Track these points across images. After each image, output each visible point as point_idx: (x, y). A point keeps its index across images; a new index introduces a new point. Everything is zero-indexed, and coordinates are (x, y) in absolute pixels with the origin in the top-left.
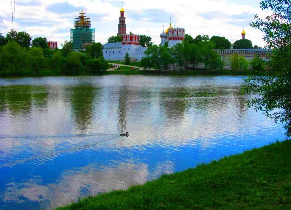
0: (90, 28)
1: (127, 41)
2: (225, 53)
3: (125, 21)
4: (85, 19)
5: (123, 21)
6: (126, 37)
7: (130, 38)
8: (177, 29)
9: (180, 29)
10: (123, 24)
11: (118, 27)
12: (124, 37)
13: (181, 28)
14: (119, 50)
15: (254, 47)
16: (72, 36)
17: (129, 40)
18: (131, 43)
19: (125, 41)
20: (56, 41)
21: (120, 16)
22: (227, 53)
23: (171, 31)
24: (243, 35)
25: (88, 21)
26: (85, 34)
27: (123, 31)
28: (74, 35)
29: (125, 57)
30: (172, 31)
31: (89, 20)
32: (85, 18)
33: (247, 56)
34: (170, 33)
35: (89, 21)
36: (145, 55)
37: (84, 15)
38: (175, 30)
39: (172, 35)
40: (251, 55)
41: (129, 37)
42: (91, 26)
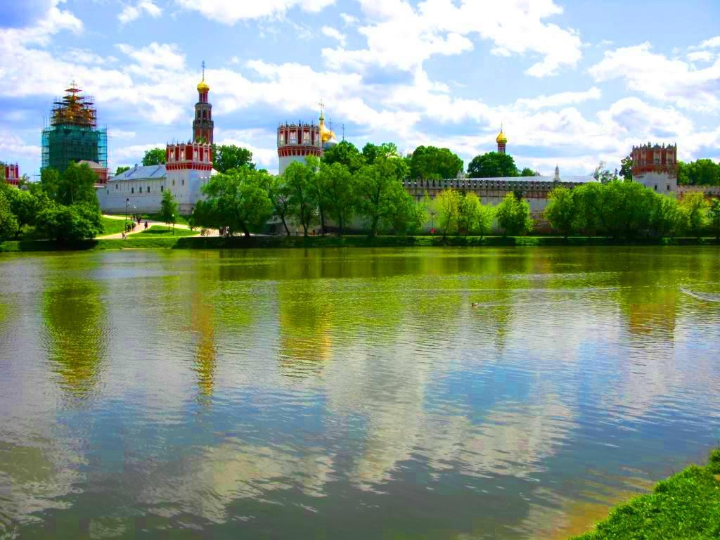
0: (94, 129)
2: (431, 187)
4: (81, 105)
5: (205, 112)
6: (177, 149)
8: (300, 125)
12: (172, 151)
16: (47, 150)
18: (189, 166)
19: (174, 161)
20: (14, 164)
21: (198, 101)
22: (437, 187)
24: (502, 144)
26: (79, 144)
29: (163, 202)
30: (286, 132)
31: (90, 107)
33: (492, 195)
36: (207, 195)
37: (76, 94)
41: (182, 150)
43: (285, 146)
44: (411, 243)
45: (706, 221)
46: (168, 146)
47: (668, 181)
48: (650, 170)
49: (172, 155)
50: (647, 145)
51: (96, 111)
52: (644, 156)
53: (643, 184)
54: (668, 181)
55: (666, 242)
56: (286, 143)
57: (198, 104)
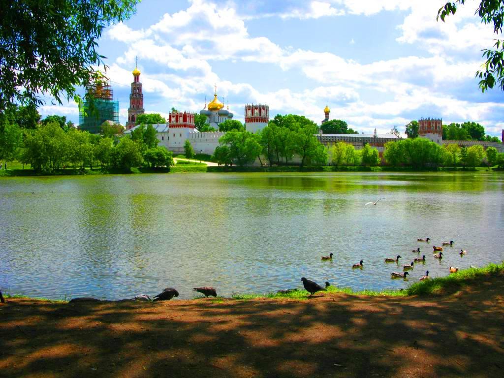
0: (111, 101)
3: (141, 88)
7: (182, 117)
9: (263, 106)
11: (131, 99)
12: (173, 117)
13: (265, 105)
15: (349, 130)
18: (185, 126)
19: (175, 123)
21: (133, 81)
22: (325, 140)
23: (251, 108)
24: (327, 114)
25: (107, 90)
26: (105, 110)
27: (138, 104)
34: (250, 112)
35: (110, 90)
38: (256, 108)
39: (252, 115)
40: (357, 144)
41: (181, 116)
42: (113, 98)
44: (321, 170)
45: (458, 159)
46: (170, 114)
47: (438, 138)
48: (429, 132)
49: (174, 119)
51: (112, 90)
53: (420, 138)
54: (438, 138)
55: (441, 170)
56: (252, 115)
57: (132, 83)
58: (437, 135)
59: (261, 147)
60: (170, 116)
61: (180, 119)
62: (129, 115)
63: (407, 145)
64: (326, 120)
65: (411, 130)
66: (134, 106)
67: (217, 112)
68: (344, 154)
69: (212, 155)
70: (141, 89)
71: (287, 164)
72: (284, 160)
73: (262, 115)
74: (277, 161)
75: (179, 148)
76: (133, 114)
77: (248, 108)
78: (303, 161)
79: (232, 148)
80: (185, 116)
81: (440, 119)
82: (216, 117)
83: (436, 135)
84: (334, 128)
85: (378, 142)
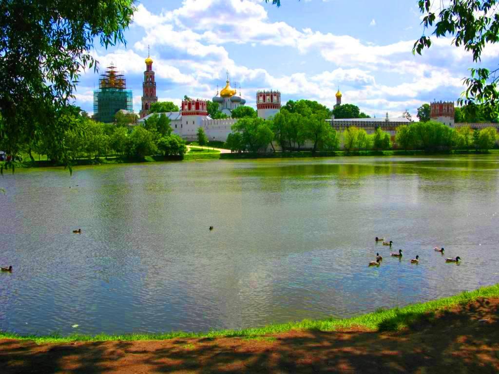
0: (124, 90)
1: (191, 111)
3: (154, 76)
4: (117, 76)
7: (195, 105)
9: (275, 92)
10: (151, 82)
11: (144, 87)
12: (186, 104)
13: (276, 91)
14: (176, 123)
16: (97, 103)
17: (193, 107)
18: (198, 114)
19: (188, 111)
21: (146, 70)
24: (339, 98)
27: (151, 92)
28: (99, 101)
32: (117, 74)
34: (261, 99)
35: (123, 80)
37: (114, 70)
39: (264, 101)
40: (369, 128)
41: (193, 104)
42: (127, 87)
43: (263, 103)
44: (333, 155)
45: (471, 142)
48: (441, 115)
49: (186, 107)
50: (440, 102)
52: (438, 108)
53: (433, 122)
54: (450, 121)
55: (453, 152)
56: (264, 101)
58: (450, 118)
59: (273, 133)
60: (183, 104)
61: (192, 107)
62: (142, 104)
63: (419, 128)
64: (338, 104)
65: (423, 113)
66: (147, 94)
67: (229, 98)
68: (356, 138)
69: (225, 142)
70: (154, 78)
71: (299, 149)
72: (297, 145)
73: (274, 101)
74: (289, 146)
75: (192, 135)
76: (146, 102)
77: (260, 95)
78: (315, 146)
79: (244, 134)
80: (197, 104)
81: (452, 102)
82: (229, 103)
83: (448, 118)
84: (346, 112)
85: (389, 125)
